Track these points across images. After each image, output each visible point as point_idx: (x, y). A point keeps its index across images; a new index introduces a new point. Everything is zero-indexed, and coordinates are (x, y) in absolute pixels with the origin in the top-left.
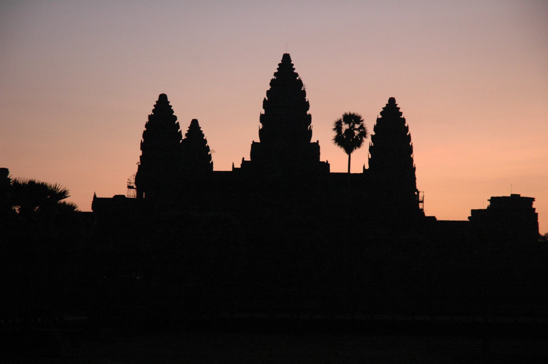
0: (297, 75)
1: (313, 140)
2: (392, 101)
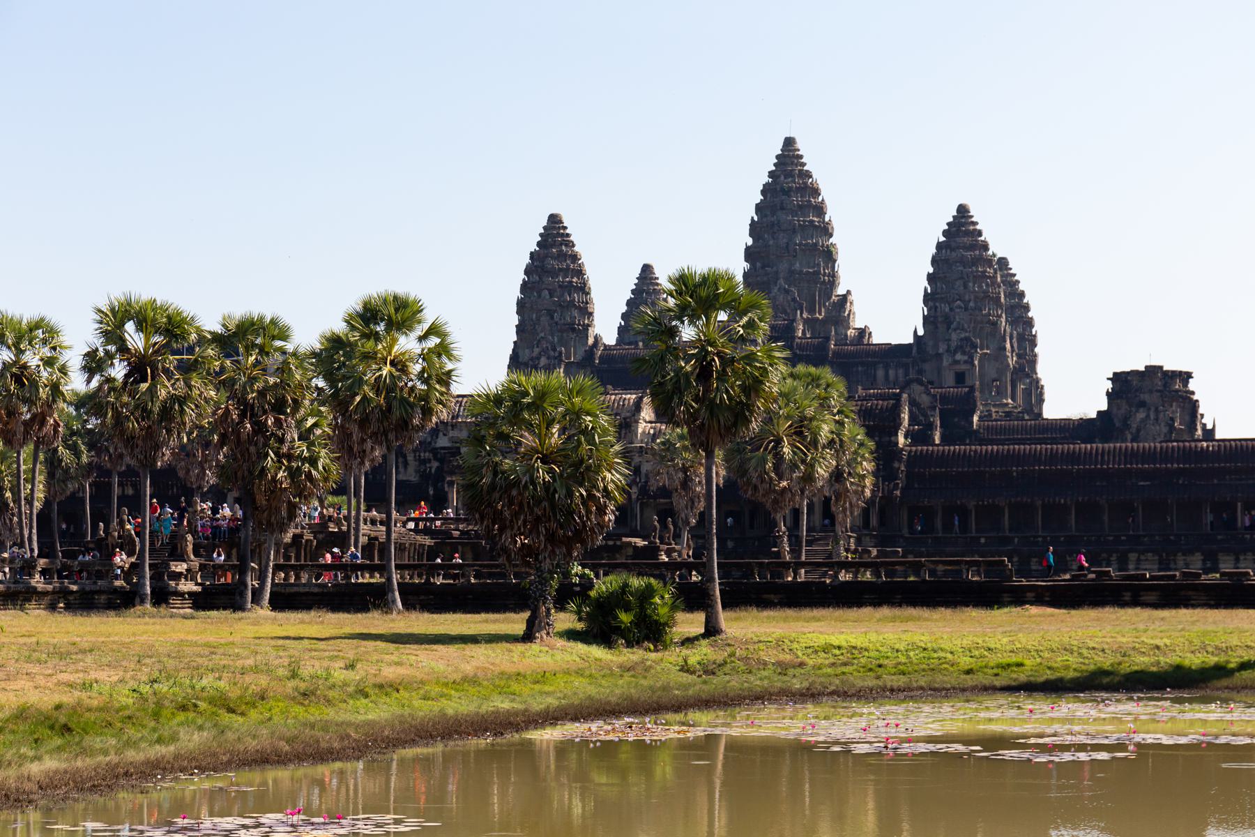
0: (808, 175)
1: (841, 290)
2: (963, 210)
